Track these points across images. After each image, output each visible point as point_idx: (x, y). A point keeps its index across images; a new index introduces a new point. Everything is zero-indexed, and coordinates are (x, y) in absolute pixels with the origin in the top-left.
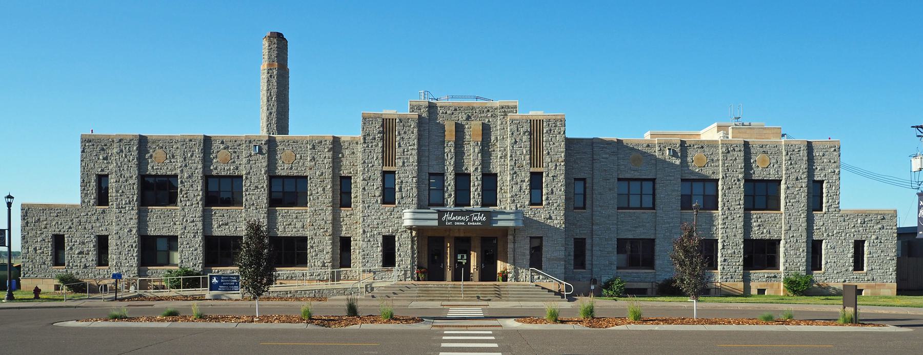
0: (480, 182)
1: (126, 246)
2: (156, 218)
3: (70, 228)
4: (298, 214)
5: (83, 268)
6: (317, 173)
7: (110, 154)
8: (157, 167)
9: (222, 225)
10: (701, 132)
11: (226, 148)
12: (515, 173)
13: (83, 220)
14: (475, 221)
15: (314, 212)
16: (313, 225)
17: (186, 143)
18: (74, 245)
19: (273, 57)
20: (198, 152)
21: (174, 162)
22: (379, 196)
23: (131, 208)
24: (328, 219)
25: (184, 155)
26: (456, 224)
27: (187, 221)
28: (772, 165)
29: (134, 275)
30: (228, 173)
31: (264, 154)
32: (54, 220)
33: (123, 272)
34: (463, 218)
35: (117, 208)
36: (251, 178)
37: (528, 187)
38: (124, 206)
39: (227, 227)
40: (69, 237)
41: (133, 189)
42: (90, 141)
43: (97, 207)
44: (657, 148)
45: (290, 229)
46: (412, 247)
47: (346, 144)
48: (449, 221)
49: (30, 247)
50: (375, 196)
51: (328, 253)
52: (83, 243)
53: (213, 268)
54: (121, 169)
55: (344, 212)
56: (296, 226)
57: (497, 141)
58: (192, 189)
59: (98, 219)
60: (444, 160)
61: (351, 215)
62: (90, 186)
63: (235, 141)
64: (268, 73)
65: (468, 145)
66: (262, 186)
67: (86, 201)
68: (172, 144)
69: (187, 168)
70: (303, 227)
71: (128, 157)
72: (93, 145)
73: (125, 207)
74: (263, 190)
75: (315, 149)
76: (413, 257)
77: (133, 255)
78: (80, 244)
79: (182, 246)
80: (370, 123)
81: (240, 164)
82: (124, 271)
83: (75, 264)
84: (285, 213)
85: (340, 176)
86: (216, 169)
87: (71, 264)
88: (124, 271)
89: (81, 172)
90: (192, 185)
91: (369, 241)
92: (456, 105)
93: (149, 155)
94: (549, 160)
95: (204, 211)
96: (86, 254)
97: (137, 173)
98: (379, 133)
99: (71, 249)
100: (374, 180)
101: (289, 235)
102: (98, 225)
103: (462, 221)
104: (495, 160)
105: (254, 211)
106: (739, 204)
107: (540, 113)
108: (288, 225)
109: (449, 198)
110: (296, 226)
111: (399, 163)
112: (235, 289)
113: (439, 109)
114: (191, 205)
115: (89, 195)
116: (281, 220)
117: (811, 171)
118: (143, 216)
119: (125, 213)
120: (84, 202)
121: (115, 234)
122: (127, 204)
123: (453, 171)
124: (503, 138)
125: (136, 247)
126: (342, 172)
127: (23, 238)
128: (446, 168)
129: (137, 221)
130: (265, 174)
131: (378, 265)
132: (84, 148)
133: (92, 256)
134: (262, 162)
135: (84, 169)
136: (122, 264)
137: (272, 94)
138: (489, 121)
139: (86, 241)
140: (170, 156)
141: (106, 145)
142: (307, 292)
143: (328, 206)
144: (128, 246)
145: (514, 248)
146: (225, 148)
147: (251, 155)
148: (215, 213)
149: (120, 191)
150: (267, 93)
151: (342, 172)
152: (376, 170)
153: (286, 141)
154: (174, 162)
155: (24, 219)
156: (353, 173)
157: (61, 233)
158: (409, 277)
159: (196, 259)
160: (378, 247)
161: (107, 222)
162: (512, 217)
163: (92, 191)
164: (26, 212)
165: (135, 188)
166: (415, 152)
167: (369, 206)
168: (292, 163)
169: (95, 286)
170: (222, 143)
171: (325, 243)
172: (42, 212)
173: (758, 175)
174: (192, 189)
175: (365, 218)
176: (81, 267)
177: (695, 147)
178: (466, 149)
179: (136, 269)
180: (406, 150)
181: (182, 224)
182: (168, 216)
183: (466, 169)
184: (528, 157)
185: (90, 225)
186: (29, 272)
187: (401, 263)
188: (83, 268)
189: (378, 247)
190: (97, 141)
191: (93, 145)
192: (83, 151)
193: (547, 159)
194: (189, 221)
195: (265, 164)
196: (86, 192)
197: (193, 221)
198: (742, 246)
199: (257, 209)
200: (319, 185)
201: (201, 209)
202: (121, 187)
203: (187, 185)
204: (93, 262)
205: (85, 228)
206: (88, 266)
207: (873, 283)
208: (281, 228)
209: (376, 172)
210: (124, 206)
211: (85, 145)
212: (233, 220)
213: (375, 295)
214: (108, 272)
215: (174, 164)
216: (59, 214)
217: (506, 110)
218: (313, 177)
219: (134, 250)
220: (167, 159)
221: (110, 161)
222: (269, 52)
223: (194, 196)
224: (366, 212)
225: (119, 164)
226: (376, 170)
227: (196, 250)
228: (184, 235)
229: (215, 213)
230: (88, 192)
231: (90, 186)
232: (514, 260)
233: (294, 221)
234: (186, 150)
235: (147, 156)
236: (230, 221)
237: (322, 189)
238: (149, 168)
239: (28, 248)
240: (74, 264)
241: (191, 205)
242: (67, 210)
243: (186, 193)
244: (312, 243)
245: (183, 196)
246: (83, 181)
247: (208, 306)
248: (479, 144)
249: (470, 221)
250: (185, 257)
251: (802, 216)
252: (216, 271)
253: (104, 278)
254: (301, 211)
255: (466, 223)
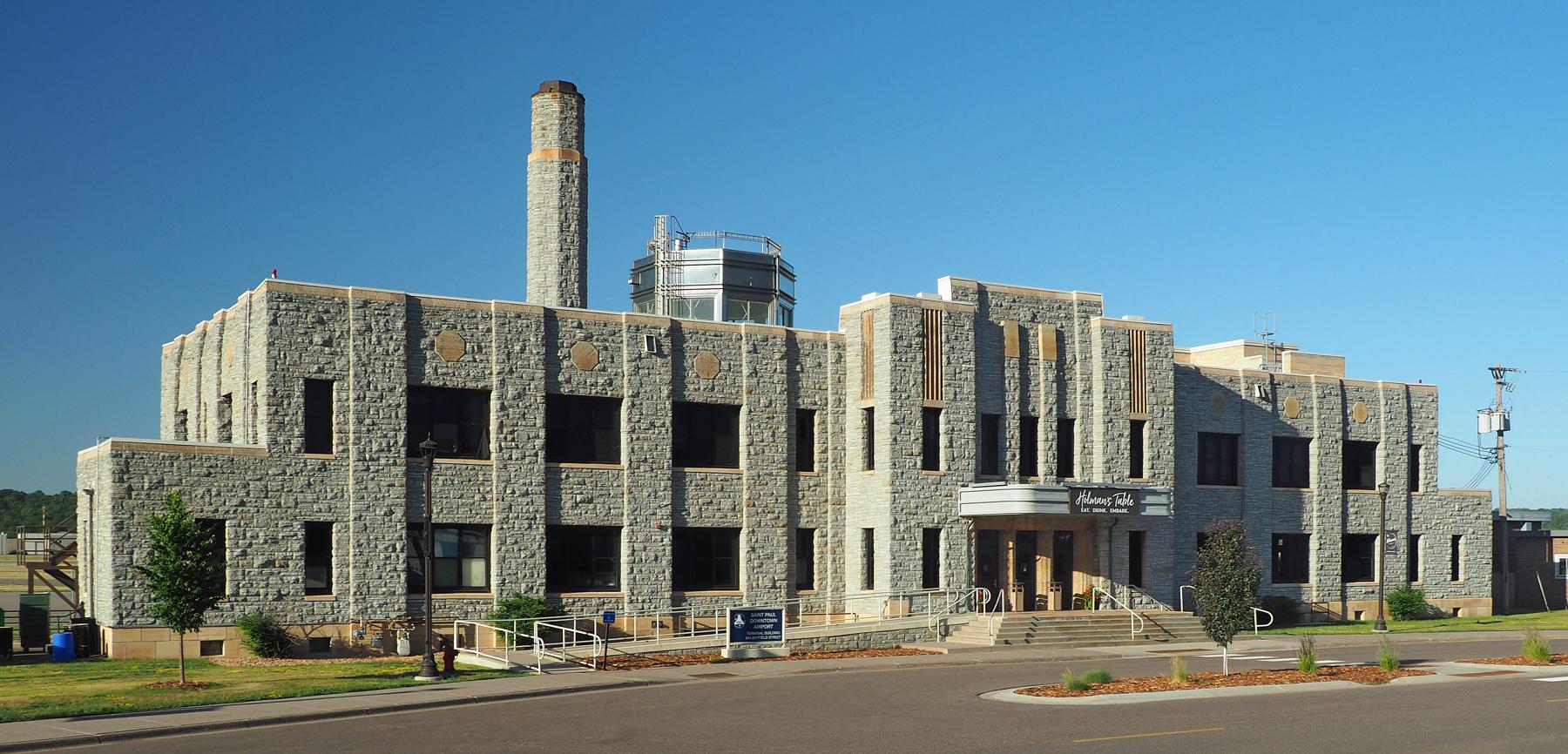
0: (1056, 434)
1: (381, 547)
2: (444, 485)
3: (242, 504)
4: (725, 483)
5: (274, 600)
6: (762, 401)
7: (337, 334)
8: (444, 370)
9: (580, 502)
10: (1192, 350)
11: (589, 338)
12: (1111, 421)
13: (273, 485)
14: (1120, 507)
15: (756, 478)
16: (754, 505)
17: (510, 322)
18: (250, 545)
19: (569, 136)
20: (534, 339)
21: (481, 361)
22: (919, 455)
23: (391, 461)
24: (781, 493)
25: (506, 347)
26: (1096, 510)
27: (513, 492)
28: (1369, 419)
29: (398, 614)
30: (594, 391)
31: (665, 356)
32: (199, 483)
33: (372, 606)
34: (1104, 501)
35: (359, 460)
36: (641, 404)
37: (1129, 447)
38: (375, 456)
39: (591, 506)
40: (239, 526)
41: (397, 417)
42: (291, 300)
43: (307, 456)
44: (1243, 386)
45: (710, 513)
46: (969, 551)
47: (807, 346)
48: (1086, 506)
49: (136, 550)
50: (912, 454)
51: (782, 560)
52: (275, 541)
53: (563, 595)
54: (369, 370)
55: (804, 479)
56: (722, 506)
57: (1076, 362)
58: (524, 423)
59: (309, 484)
60: (1003, 391)
61: (816, 486)
62: (289, 404)
63: (605, 325)
64: (562, 170)
65: (1035, 367)
66: (662, 422)
67: (281, 439)
68: (474, 321)
69: (515, 375)
70: (734, 509)
71: (384, 343)
72: (298, 309)
73: (378, 459)
74: (664, 432)
75: (756, 353)
76: (970, 570)
77: (395, 570)
78: (266, 542)
79: (503, 548)
80: (904, 315)
81: (616, 375)
82: (375, 604)
83: (253, 591)
84: (702, 479)
85: (797, 409)
86: (568, 381)
87: (242, 591)
88: (375, 604)
89: (268, 370)
90: (525, 414)
91: (903, 539)
92: (1014, 291)
93: (428, 340)
94: (1155, 401)
95: (547, 470)
96: (281, 566)
97: (405, 381)
98: (918, 335)
99: (244, 554)
100: (910, 424)
101: (709, 525)
102: (310, 497)
103: (1101, 506)
104: (1073, 396)
105: (648, 475)
106: (1337, 479)
107: (1140, 319)
108: (708, 504)
109: (1012, 460)
110: (722, 506)
111: (948, 393)
112: (775, 637)
113: (990, 296)
114: (522, 459)
115: (288, 427)
116: (694, 493)
117: (1410, 437)
118: (416, 480)
119: (377, 471)
120: (276, 443)
121: (355, 519)
122: (383, 450)
123: (1018, 413)
124: (1086, 358)
125: (402, 550)
126: (800, 401)
127: (119, 527)
128: (1008, 406)
129: (403, 490)
130: (668, 397)
131: (916, 586)
132: (275, 315)
133: (295, 572)
134: (662, 372)
135: (276, 364)
136: (371, 589)
137: (570, 216)
138: (1062, 327)
139: (281, 535)
140: (473, 347)
141: (327, 312)
142: (846, 638)
143: (781, 468)
144: (386, 549)
145: (1110, 550)
146: (586, 339)
147: (640, 358)
148: (568, 477)
149: (367, 421)
150: (560, 213)
151: (800, 401)
152: (913, 405)
153: (700, 332)
154: (481, 361)
155: (121, 480)
156: (819, 403)
157: (219, 516)
158: (964, 606)
159: (533, 576)
160: (917, 549)
161: (332, 491)
162: (1163, 499)
163: (294, 418)
164: (127, 464)
165: (400, 415)
166: (971, 375)
167: (902, 473)
168: (714, 378)
169: (299, 640)
170: (580, 326)
171: (775, 542)
172: (167, 463)
173: (1354, 435)
174: (524, 423)
175: (897, 495)
176: (270, 597)
177: (1286, 385)
178: (1032, 373)
179: (403, 599)
180: (958, 371)
181: (503, 500)
182: (470, 481)
183: (1034, 410)
184: (1127, 393)
185: (291, 499)
186: (133, 612)
187: (951, 579)
188: (274, 600)
189: (917, 549)
190: (305, 300)
191: (298, 309)
192: (274, 323)
193: (1151, 399)
194: (518, 493)
195: (668, 378)
196: (281, 418)
197: (526, 494)
198: (1340, 545)
199: (652, 470)
200: (765, 425)
201: (543, 467)
202: (369, 412)
203: (514, 413)
204: (298, 586)
205: (279, 505)
206: (285, 595)
207: (1469, 599)
208: (693, 511)
209: (913, 409)
210: (375, 456)
211: (278, 308)
212: (603, 492)
213: (1009, 639)
214: (333, 607)
215: (481, 365)
216: (212, 470)
217: (1089, 308)
218: (755, 409)
219: (398, 556)
220: (466, 353)
221: (338, 350)
222: (561, 125)
223: (529, 438)
224: (897, 483)
225: (364, 359)
226: (913, 405)
227: (533, 556)
228: (507, 523)
229: (568, 477)
230: (287, 419)
231: (289, 404)
232: (1110, 570)
233: (718, 495)
234: (509, 336)
235: (424, 343)
236: (596, 493)
237: (770, 433)
238: (428, 370)
239: (132, 553)
240: (250, 590)
241: (522, 459)
242: (233, 460)
243: (512, 432)
244: (753, 540)
245: (505, 438)
246: (275, 392)
247: (834, 670)
248: (1054, 367)
249: (1113, 506)
250: (509, 571)
251: (1403, 499)
252: (571, 600)
253: (323, 623)
254: (728, 477)
255: (1108, 509)
